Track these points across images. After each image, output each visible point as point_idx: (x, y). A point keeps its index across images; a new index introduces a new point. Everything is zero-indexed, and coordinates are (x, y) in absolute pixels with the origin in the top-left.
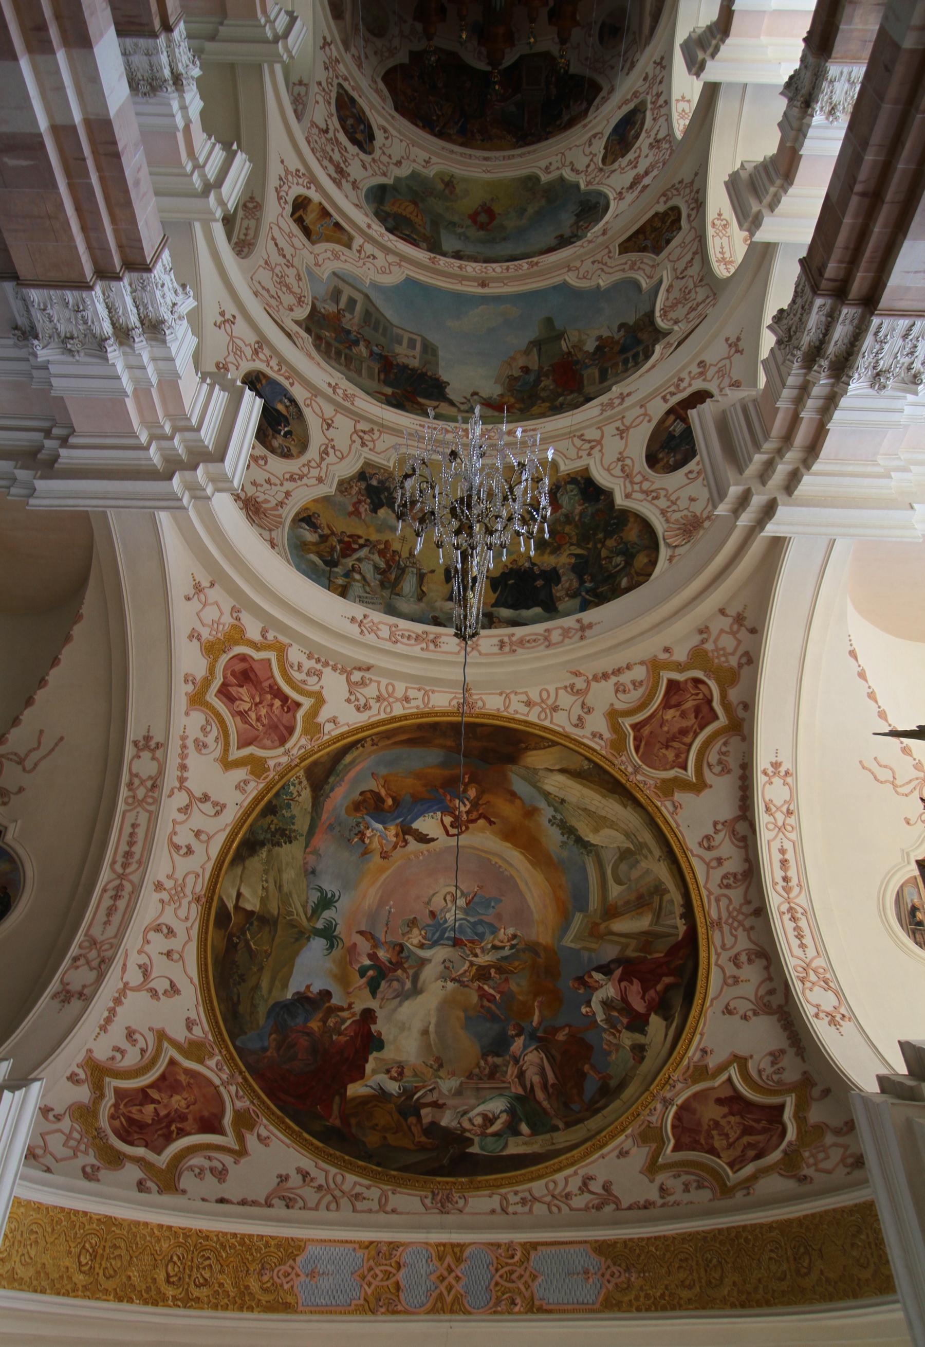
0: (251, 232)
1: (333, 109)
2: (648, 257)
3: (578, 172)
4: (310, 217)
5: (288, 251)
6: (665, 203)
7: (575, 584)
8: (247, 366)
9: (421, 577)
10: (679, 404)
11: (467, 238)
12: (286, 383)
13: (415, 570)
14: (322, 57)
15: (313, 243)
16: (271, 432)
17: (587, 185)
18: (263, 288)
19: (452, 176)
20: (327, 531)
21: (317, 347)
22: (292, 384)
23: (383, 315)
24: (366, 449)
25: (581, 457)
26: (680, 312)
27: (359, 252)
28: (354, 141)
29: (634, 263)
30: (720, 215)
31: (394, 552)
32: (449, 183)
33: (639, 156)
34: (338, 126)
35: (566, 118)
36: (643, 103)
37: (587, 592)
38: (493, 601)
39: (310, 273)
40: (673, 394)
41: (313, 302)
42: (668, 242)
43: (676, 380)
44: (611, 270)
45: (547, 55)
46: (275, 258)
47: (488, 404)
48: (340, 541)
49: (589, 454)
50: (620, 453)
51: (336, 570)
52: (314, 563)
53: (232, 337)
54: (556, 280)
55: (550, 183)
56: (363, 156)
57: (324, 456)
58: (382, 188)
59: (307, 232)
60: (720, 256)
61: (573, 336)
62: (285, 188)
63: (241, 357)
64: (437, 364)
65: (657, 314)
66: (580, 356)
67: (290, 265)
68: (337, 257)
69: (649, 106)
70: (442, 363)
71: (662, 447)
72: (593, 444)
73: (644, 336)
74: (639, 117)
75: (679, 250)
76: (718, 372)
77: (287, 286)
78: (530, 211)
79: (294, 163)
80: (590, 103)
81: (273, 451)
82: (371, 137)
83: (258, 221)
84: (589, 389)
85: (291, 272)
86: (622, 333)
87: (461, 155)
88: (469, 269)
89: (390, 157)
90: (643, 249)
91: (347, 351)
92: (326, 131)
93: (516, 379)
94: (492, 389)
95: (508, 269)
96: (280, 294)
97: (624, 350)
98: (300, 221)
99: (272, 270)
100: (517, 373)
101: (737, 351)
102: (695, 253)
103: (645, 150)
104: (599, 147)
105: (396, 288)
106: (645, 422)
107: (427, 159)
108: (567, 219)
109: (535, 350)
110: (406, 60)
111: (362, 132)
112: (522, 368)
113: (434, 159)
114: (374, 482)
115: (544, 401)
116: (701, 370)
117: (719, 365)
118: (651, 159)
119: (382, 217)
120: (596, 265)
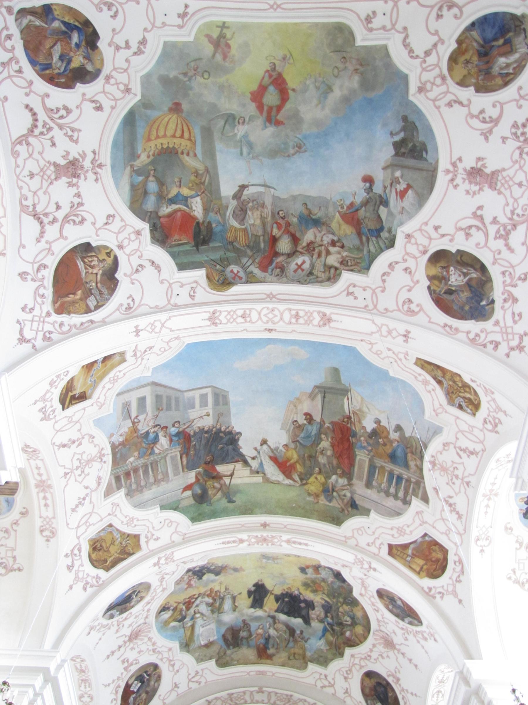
1: (29, 72)
3: (411, 51)
7: (323, 615)
9: (234, 598)
11: (250, 146)
13: (230, 596)
16: (128, 604)
17: (421, 89)
19: (224, 26)
20: (175, 605)
31: (216, 592)
33: (496, 121)
37: (328, 624)
38: (276, 608)
39: (98, 423)
42: (460, 407)
48: (184, 604)
51: (186, 620)
52: (174, 626)
55: (368, 48)
65: (427, 457)
66: (357, 428)
70: (233, 410)
78: (337, 93)
88: (254, 316)
89: (127, 46)
90: (440, 382)
91: (152, 458)
93: (300, 427)
100: (302, 420)
105: (179, 357)
107: (181, 10)
109: (319, 397)
111: (78, 46)
112: (306, 414)
114: (197, 569)
115: (320, 472)
120: (390, 354)
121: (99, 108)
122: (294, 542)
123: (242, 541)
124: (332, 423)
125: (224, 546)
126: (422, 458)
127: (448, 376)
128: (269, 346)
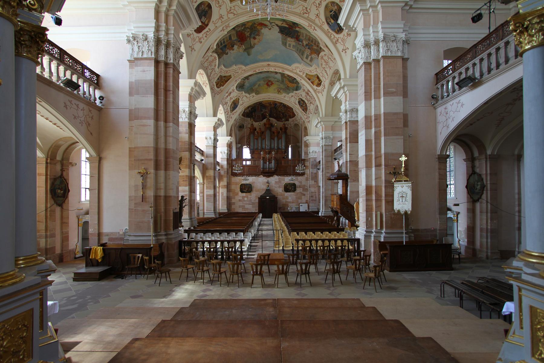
0: (333, 77)
2: (223, 75)
3: (245, 96)
4: (317, 81)
5: (324, 72)
6: (221, 89)
8: (341, 35)
10: (205, 28)
11: (274, 78)
12: (331, 31)
14: (310, 119)
15: (317, 74)
16: (337, 12)
18: (332, 61)
19: (278, 94)
21: (319, 43)
22: (328, 30)
23: (298, 54)
24: (306, 6)
25: (233, 6)
26: (211, 59)
27: (304, 73)
28: (303, 101)
29: (227, 73)
30: (206, 87)
32: (279, 92)
34: (307, 104)
35: (250, 108)
36: (231, 112)
39: (318, 66)
40: (207, 32)
41: (318, 57)
42: (218, 79)
43: (208, 36)
44: (233, 70)
45: (256, 121)
46: (328, 70)
47: (265, 26)
49: (231, 8)
50: (220, 9)
53: (344, 45)
54: (248, 67)
56: (302, 98)
57: (320, 3)
58: (297, 90)
59: (318, 77)
60: (203, 75)
61: (241, 50)
62: (322, 89)
63: (342, 38)
64: (282, 39)
65: (217, 58)
66: (238, 43)
67: (324, 68)
68: (310, 71)
69: (229, 112)
70: (281, 39)
71: (207, 11)
72: (230, 12)
73: (220, 51)
74: (231, 109)
75: (215, 77)
76: (195, 40)
77: (325, 62)
79: (320, 95)
80: (244, 112)
81: (337, 4)
82: (299, 102)
83: (331, 80)
84: (234, 32)
85: (324, 66)
86: (227, 52)
87: (276, 99)
88: (273, 69)
90: (225, 77)
92: (310, 103)
94: (264, 31)
95: (262, 70)
96: (328, 59)
97: (225, 46)
98: (320, 80)
99: (329, 66)
100: (257, 37)
101: (191, 47)
102: (210, 76)
103: (229, 102)
104: (241, 102)
105: (294, 62)
106: (214, 21)
108: (247, 84)
109: (252, 45)
110: (290, 119)
113: (283, 97)
115: (248, 27)
116: (201, 40)
117: (195, 42)
118: (227, 100)
119: (297, 83)
121: (301, 95)
122: (255, 15)
123: (279, 15)
124: (247, 40)
125: (287, 15)
126: (218, 55)
127: (224, 82)
128: (269, 58)
